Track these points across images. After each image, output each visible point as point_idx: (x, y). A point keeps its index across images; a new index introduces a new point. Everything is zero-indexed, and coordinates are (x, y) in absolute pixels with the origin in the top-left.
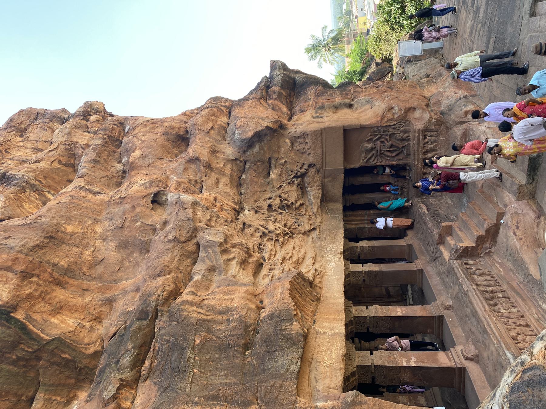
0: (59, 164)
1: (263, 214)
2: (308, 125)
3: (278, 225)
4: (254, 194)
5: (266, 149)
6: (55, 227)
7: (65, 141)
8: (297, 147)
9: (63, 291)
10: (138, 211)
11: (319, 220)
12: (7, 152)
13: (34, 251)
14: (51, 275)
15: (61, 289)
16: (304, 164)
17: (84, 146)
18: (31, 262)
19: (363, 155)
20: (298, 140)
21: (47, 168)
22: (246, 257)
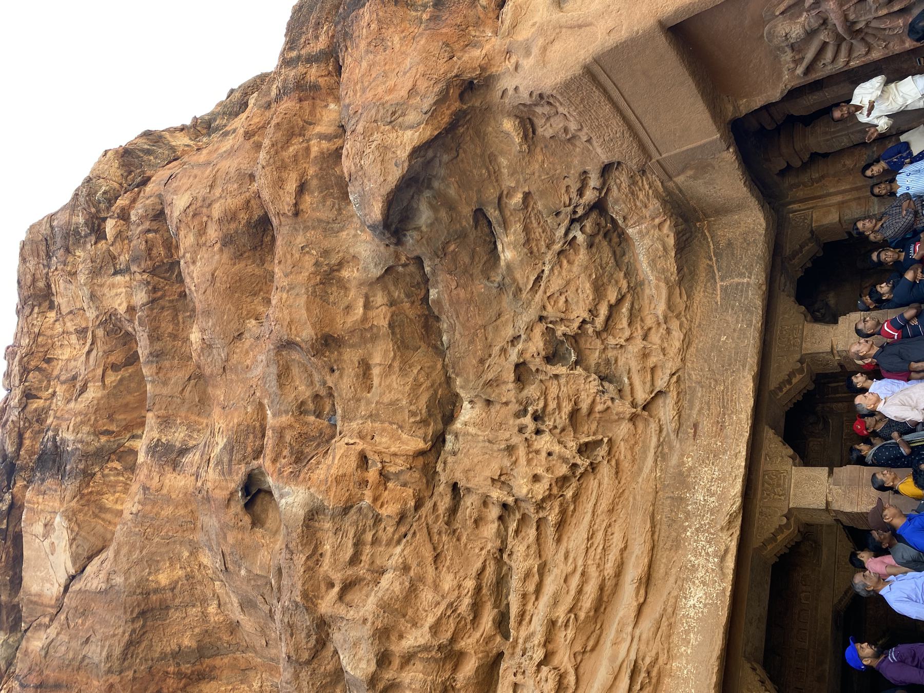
0: (116, 371)
1: (506, 404)
2: (544, 49)
3: (545, 442)
4: (472, 342)
5: (452, 192)
6: (138, 591)
7: (97, 317)
8: (545, 130)
9: (213, 684)
10: (231, 542)
11: (677, 335)
12: (49, 361)
13: (129, 656)
14: (180, 675)
15: (208, 682)
16: (585, 172)
17: (128, 318)
18: (134, 679)
19: (788, 56)
20: (539, 110)
21: (102, 398)
22: (443, 683)
